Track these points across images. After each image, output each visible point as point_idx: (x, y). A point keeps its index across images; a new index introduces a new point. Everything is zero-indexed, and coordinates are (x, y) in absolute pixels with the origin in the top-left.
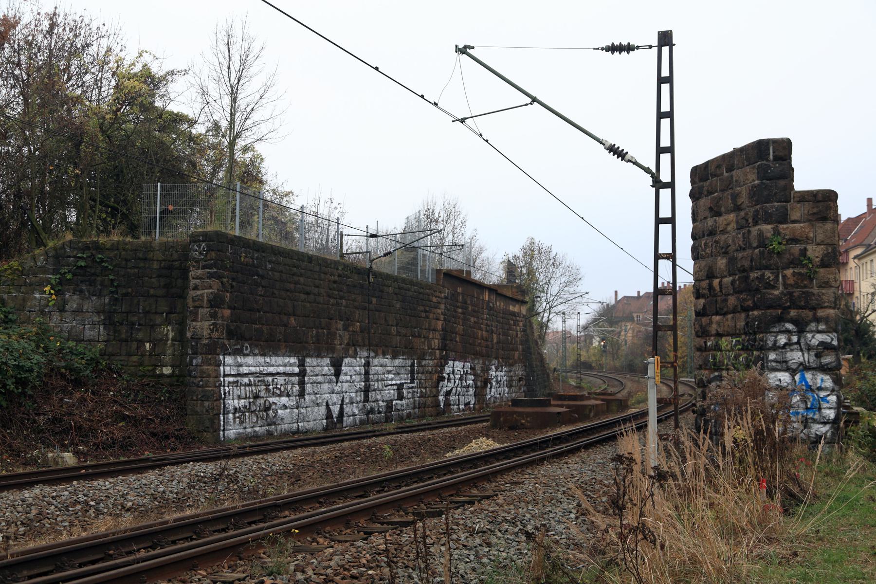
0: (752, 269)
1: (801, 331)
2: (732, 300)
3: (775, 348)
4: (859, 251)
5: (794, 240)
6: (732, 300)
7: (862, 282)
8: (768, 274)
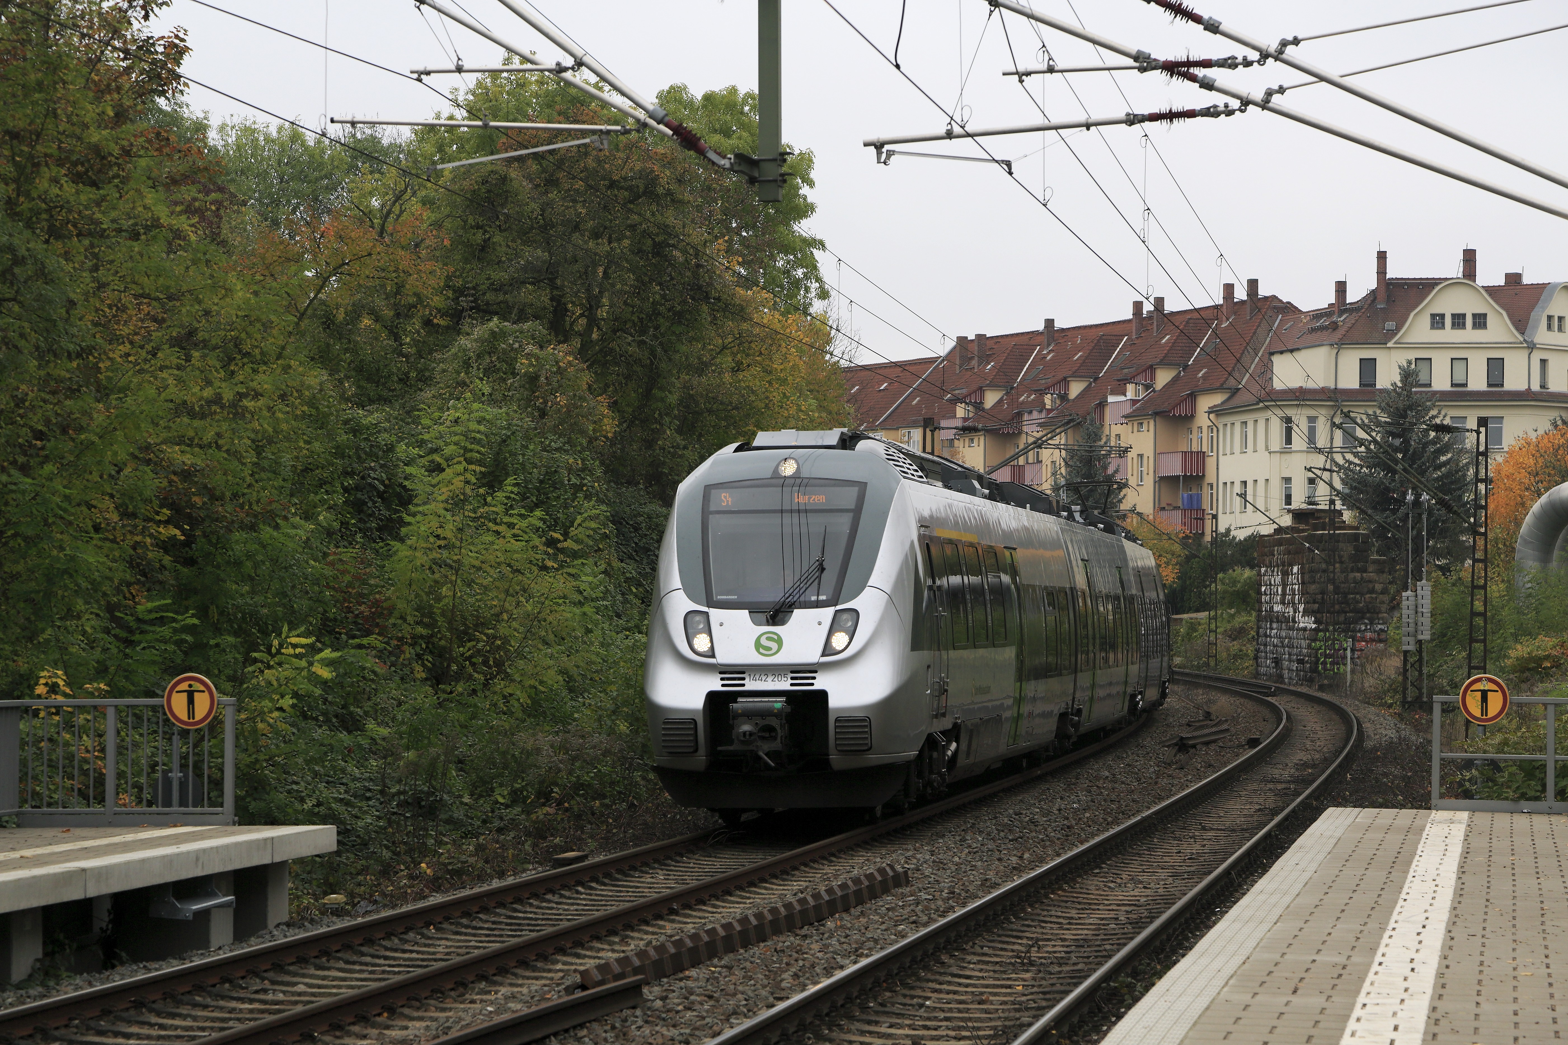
0: (1350, 593)
1: (1371, 623)
2: (1337, 607)
3: (1360, 631)
4: (1217, 399)
5: (1370, 581)
6: (1337, 607)
7: (1221, 457)
8: (1358, 596)
